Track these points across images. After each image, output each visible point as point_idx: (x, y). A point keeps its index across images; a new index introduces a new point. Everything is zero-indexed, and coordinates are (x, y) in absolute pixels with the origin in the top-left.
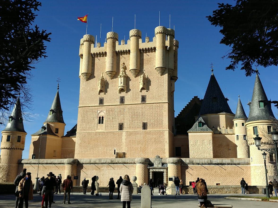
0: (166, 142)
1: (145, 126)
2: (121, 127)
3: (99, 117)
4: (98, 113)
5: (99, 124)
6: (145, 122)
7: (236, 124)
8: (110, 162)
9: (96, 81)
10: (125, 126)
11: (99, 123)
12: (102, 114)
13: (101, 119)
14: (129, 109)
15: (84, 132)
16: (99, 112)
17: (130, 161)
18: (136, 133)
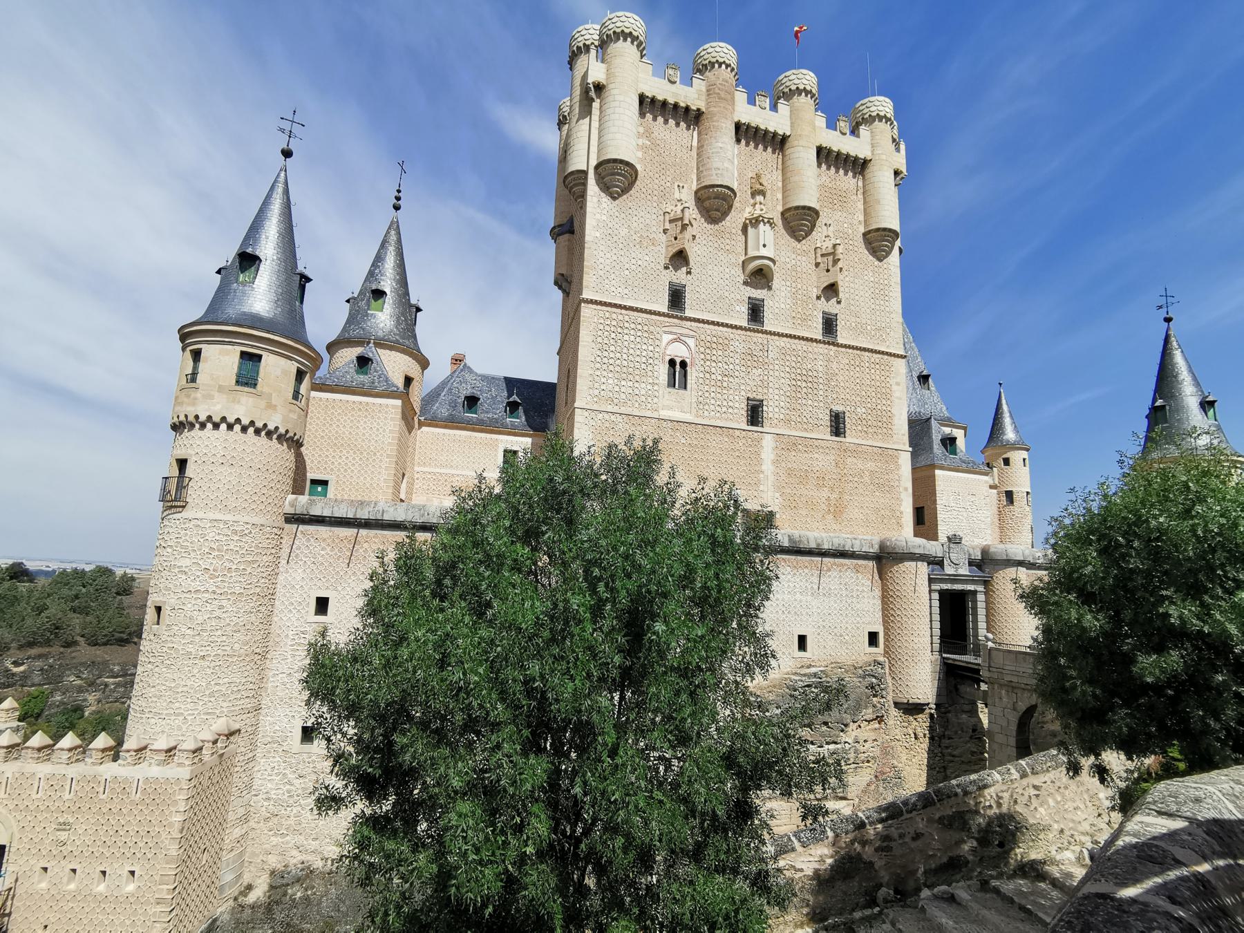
0: (906, 489)
1: (837, 424)
2: (755, 414)
3: (668, 358)
4: (664, 343)
5: (671, 390)
6: (839, 408)
7: (1007, 462)
8: (786, 544)
9: (654, 211)
10: (769, 411)
11: (672, 384)
12: (679, 352)
13: (678, 366)
14: (783, 352)
15: (610, 408)
16: (667, 338)
17: (862, 545)
18: (809, 444)
